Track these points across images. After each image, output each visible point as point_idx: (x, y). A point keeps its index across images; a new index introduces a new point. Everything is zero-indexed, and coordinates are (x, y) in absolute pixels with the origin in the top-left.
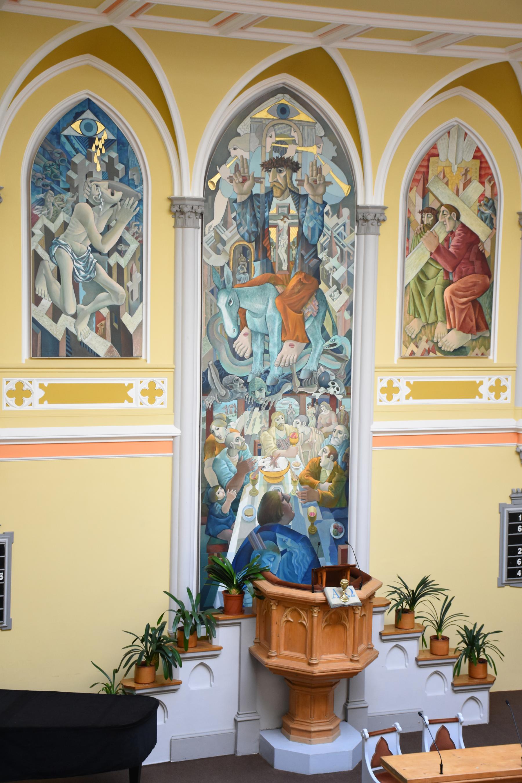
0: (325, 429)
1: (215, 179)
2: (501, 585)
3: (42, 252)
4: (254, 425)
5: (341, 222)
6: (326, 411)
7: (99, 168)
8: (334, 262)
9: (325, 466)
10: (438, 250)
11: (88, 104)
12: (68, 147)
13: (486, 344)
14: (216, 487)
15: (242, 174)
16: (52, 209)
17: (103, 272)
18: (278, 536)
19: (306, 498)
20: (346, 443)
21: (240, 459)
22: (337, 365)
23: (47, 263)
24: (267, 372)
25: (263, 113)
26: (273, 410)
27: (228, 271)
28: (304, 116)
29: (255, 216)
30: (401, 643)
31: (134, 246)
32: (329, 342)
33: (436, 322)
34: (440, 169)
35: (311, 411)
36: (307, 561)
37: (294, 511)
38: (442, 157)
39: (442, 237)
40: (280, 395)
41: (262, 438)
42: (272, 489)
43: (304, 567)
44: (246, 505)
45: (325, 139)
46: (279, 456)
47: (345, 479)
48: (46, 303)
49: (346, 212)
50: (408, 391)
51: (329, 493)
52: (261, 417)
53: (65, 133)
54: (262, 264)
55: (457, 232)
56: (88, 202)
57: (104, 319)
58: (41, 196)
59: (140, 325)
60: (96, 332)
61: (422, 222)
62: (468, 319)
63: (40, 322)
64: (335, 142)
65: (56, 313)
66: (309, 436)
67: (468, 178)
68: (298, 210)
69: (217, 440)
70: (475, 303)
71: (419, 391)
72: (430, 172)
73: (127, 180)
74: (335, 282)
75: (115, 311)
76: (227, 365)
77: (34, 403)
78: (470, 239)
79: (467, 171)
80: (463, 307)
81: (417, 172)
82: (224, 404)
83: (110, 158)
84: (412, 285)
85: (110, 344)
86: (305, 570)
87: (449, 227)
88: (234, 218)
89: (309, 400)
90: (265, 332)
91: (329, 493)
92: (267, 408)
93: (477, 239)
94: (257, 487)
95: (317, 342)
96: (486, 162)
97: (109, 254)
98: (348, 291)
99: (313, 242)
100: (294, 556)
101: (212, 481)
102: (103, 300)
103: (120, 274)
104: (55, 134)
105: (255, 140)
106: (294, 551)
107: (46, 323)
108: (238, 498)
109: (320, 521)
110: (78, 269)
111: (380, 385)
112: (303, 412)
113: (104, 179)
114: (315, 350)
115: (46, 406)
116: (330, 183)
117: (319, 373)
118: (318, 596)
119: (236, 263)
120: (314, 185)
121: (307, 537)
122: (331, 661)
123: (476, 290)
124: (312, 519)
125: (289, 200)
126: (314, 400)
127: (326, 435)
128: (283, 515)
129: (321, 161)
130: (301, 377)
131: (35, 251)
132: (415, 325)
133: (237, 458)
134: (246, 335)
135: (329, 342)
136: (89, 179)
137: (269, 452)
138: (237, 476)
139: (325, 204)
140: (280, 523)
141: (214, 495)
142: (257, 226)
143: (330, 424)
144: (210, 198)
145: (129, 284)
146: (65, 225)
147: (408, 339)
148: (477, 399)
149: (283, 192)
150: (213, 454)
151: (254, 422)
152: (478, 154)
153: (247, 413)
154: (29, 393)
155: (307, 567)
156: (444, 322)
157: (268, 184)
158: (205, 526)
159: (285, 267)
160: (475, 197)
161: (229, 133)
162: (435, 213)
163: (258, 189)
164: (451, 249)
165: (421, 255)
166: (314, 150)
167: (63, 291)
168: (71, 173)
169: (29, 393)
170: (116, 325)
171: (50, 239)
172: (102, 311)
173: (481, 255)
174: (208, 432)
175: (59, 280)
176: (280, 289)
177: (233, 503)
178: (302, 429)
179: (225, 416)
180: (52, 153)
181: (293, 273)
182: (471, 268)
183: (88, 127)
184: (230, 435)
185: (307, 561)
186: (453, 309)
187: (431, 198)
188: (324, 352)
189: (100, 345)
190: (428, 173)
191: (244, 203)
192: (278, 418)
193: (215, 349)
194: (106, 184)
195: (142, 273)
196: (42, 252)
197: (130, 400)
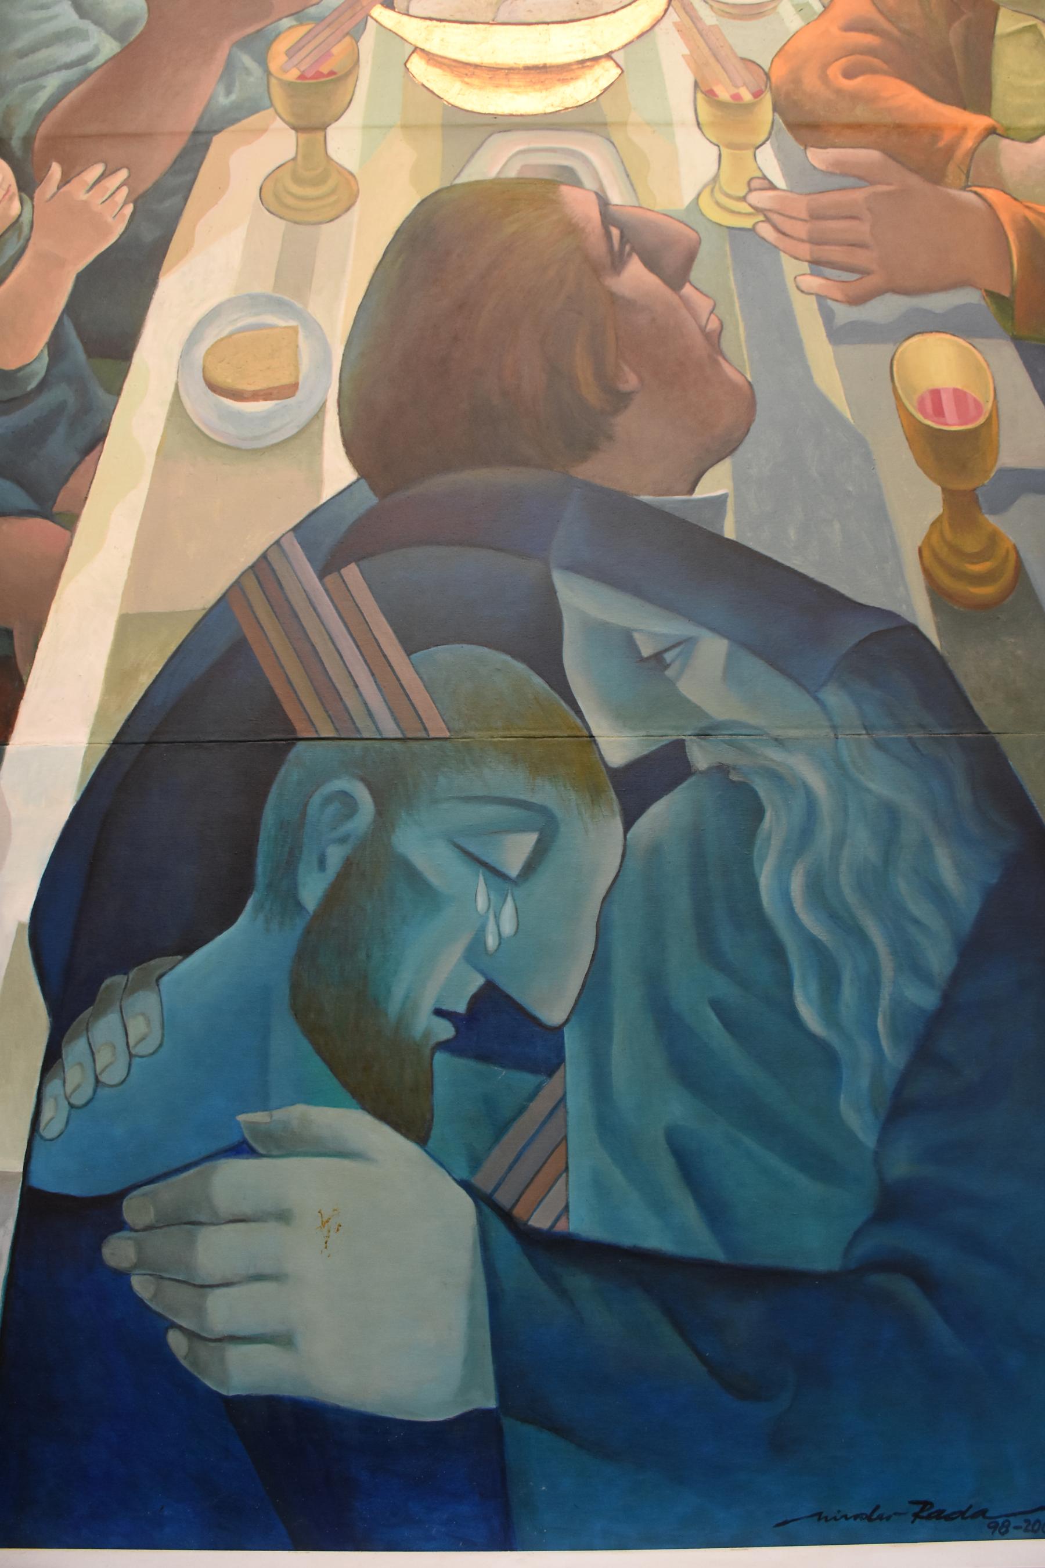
18: (579, 600)
19: (861, 258)
36: (936, 892)
37: (741, 357)
42: (494, 162)
43: (911, 964)
44: (221, 292)
86: (925, 998)
94: (344, 143)
100: (776, 826)
106: (775, 776)
108: (149, 234)
121: (915, 629)
124: (953, 450)
128: (620, 400)
140: (601, 470)
155: (939, 958)
177: (79, 277)
185: (936, 892)
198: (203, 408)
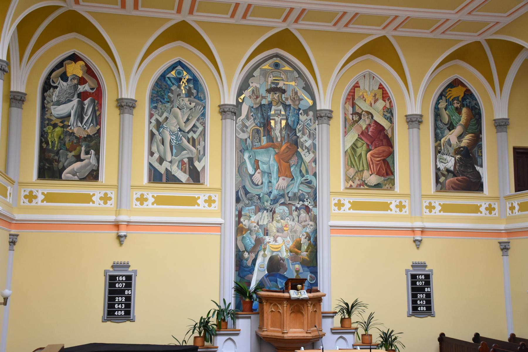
0: (303, 224)
1: (242, 97)
2: (410, 316)
3: (155, 131)
4: (264, 220)
5: (308, 118)
6: (303, 214)
7: (184, 92)
8: (305, 138)
9: (304, 243)
10: (362, 133)
11: (179, 63)
12: (169, 82)
13: (392, 182)
14: (244, 252)
15: (255, 94)
16: (160, 111)
17: (185, 141)
18: (278, 279)
20: (315, 231)
21: (256, 237)
22: (309, 190)
23: (157, 136)
24: (271, 192)
25: (266, 66)
26: (274, 212)
27: (249, 141)
28: (287, 68)
29: (263, 115)
30: (344, 336)
31: (201, 128)
32: (304, 178)
33: (364, 170)
34: (361, 94)
35: (295, 214)
37: (287, 266)
38: (362, 88)
39: (364, 128)
40: (278, 204)
41: (269, 226)
42: (274, 254)
45: (299, 79)
46: (278, 236)
47: (315, 251)
48: (156, 155)
49: (311, 113)
50: (350, 206)
51: (307, 258)
52: (267, 216)
53: (168, 76)
54: (267, 139)
55: (372, 125)
56: (178, 107)
57: (186, 164)
58: (155, 105)
59: (204, 168)
60: (181, 170)
61: (353, 119)
62: (381, 169)
63: (153, 165)
64: (304, 80)
65: (161, 160)
66: (294, 227)
67: (377, 98)
68: (285, 112)
69: (244, 226)
70: (384, 161)
71: (355, 206)
72: (356, 95)
73: (197, 97)
74: (306, 148)
75: (191, 160)
76: (249, 188)
77: (149, 204)
78: (380, 128)
79: (375, 95)
80: (378, 163)
81: (348, 95)
82: (247, 208)
83: (189, 87)
84: (349, 151)
85: (187, 176)
87: (367, 123)
88: (252, 116)
89: (294, 208)
90: (269, 172)
91: (307, 258)
92: (271, 211)
93: (383, 128)
94: (266, 252)
95: (297, 178)
96: (386, 91)
97: (188, 132)
98: (313, 152)
99: (294, 128)
101: (242, 248)
102: (185, 154)
103: (193, 142)
104: (163, 76)
105: (262, 79)
107: (156, 165)
109: (302, 273)
110: (173, 139)
111: (333, 202)
112: (291, 214)
113: (186, 97)
114: (297, 182)
115: (155, 206)
116: (302, 99)
117: (299, 194)
118: (286, 295)
119: (253, 137)
120: (293, 100)
122: (295, 332)
123: (385, 154)
124: (297, 271)
125: (281, 107)
126: (297, 208)
127: (304, 227)
129: (297, 89)
130: (289, 195)
131: (151, 131)
132: (352, 172)
133: (255, 236)
134: (259, 173)
135: (304, 178)
136: (179, 97)
137: (272, 234)
138: (255, 246)
139: (299, 109)
140: (280, 272)
141: (243, 256)
142: (264, 119)
143: (306, 221)
144: (239, 106)
145: (198, 147)
146: (167, 118)
147: (348, 179)
148: (389, 212)
149: (277, 103)
150: (242, 234)
151: (264, 218)
152: (381, 87)
153: (260, 213)
154: (146, 200)
156: (368, 170)
157: (269, 100)
158: (237, 272)
159: (279, 140)
160: (381, 107)
161: (250, 75)
162: (360, 115)
163: (264, 102)
164: (369, 133)
165: (353, 136)
166: (293, 83)
167: (165, 150)
168: (170, 94)
169: (146, 200)
170: (191, 167)
171: (159, 125)
172: (184, 160)
173: (386, 136)
174: (238, 222)
175: (163, 144)
176: (277, 151)
178: (290, 223)
179: (248, 214)
180: (161, 85)
181: (284, 143)
182: (381, 143)
183: (179, 73)
184: (251, 224)
186: (373, 164)
187: (357, 107)
188: (302, 183)
189: (183, 177)
190: (354, 95)
191: (257, 108)
192: (277, 217)
193: (242, 180)
194: (187, 99)
195: (205, 141)
196: (155, 131)
197: (199, 205)
198: (260, 268)
